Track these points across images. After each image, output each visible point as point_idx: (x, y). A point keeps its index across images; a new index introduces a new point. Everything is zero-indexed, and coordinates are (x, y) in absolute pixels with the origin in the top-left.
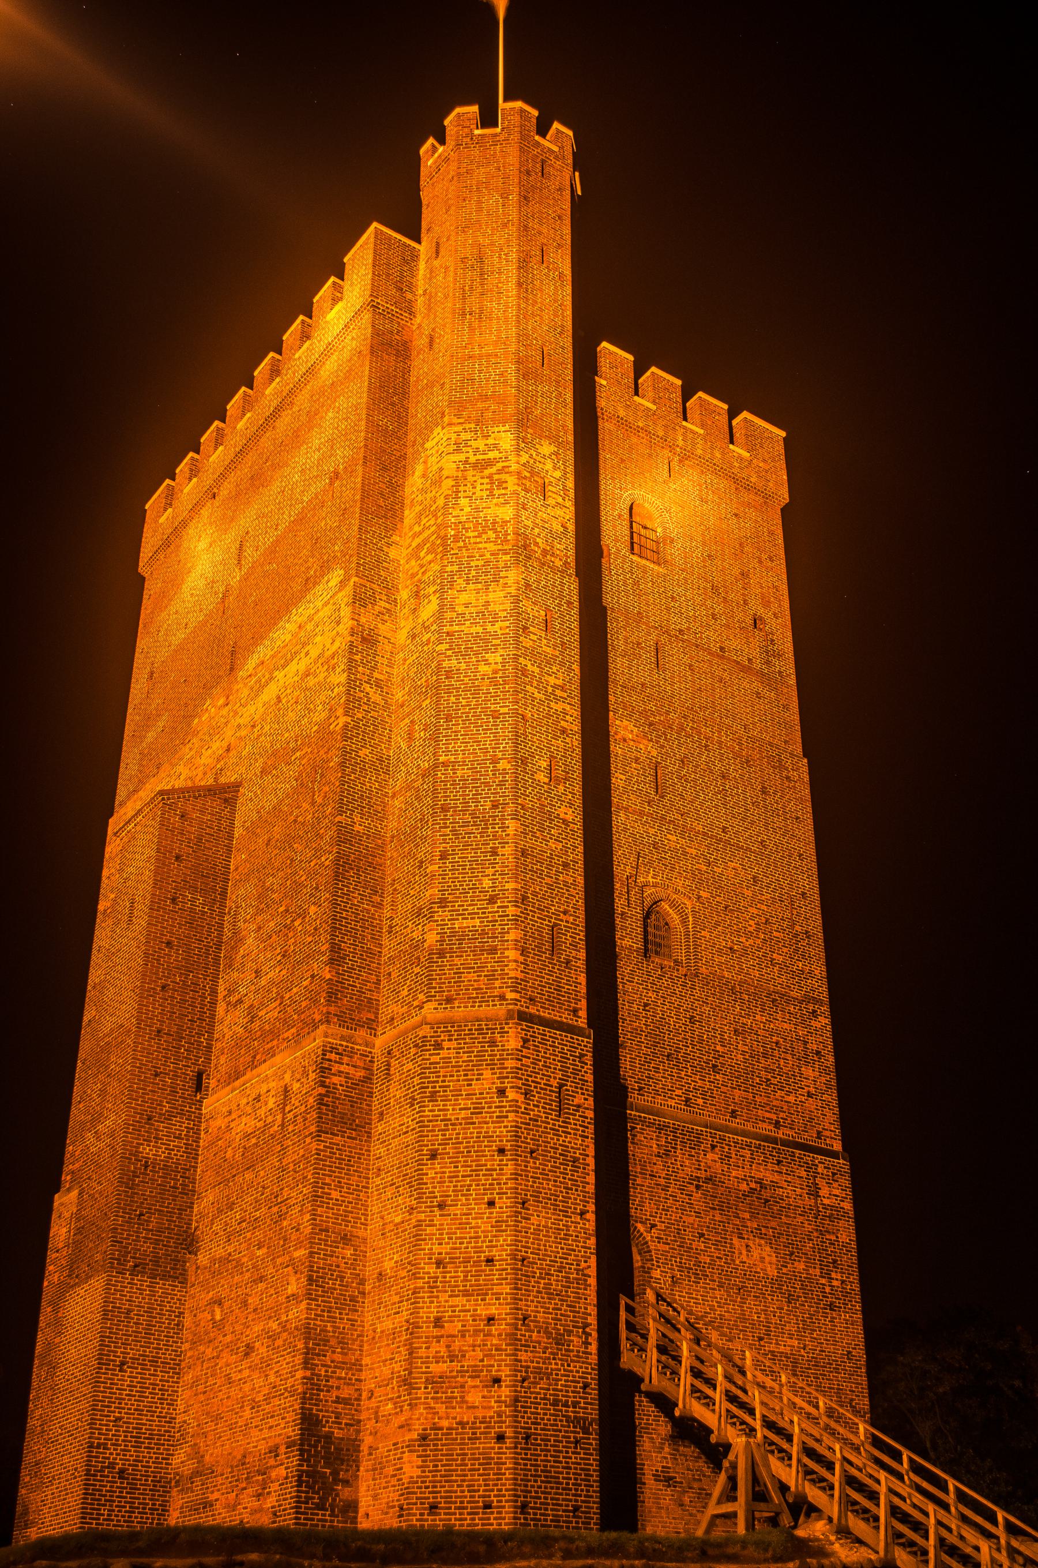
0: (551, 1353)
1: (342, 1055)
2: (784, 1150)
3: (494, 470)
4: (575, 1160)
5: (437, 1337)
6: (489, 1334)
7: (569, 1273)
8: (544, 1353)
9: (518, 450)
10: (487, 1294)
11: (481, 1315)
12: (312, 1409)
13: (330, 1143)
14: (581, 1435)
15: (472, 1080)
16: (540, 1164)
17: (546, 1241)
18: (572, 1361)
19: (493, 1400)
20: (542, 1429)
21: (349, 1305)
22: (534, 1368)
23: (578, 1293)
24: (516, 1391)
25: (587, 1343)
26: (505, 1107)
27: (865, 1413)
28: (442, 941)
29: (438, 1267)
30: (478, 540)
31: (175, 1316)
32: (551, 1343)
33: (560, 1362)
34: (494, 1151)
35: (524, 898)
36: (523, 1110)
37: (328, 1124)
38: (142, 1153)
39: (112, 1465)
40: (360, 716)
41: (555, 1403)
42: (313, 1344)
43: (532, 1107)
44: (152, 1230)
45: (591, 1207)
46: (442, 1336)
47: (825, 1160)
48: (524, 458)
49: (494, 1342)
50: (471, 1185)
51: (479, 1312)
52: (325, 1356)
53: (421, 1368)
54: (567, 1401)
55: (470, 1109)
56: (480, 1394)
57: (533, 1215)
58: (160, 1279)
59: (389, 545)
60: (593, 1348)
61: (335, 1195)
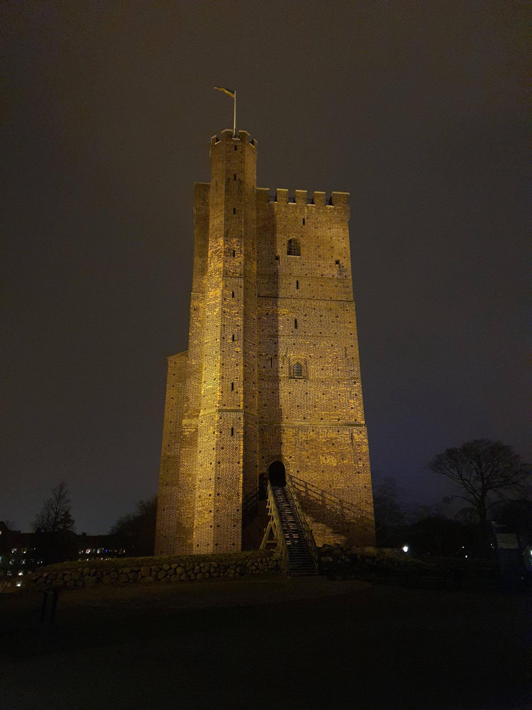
2: (340, 427)
3: (218, 253)
4: (236, 448)
5: (199, 501)
9: (224, 245)
10: (209, 488)
16: (224, 451)
18: (233, 504)
20: (223, 523)
24: (214, 514)
27: (371, 504)
39: (163, 535)
40: (194, 332)
45: (241, 460)
47: (357, 428)
48: (227, 246)
59: (203, 279)
60: (241, 499)
61: (186, 464)
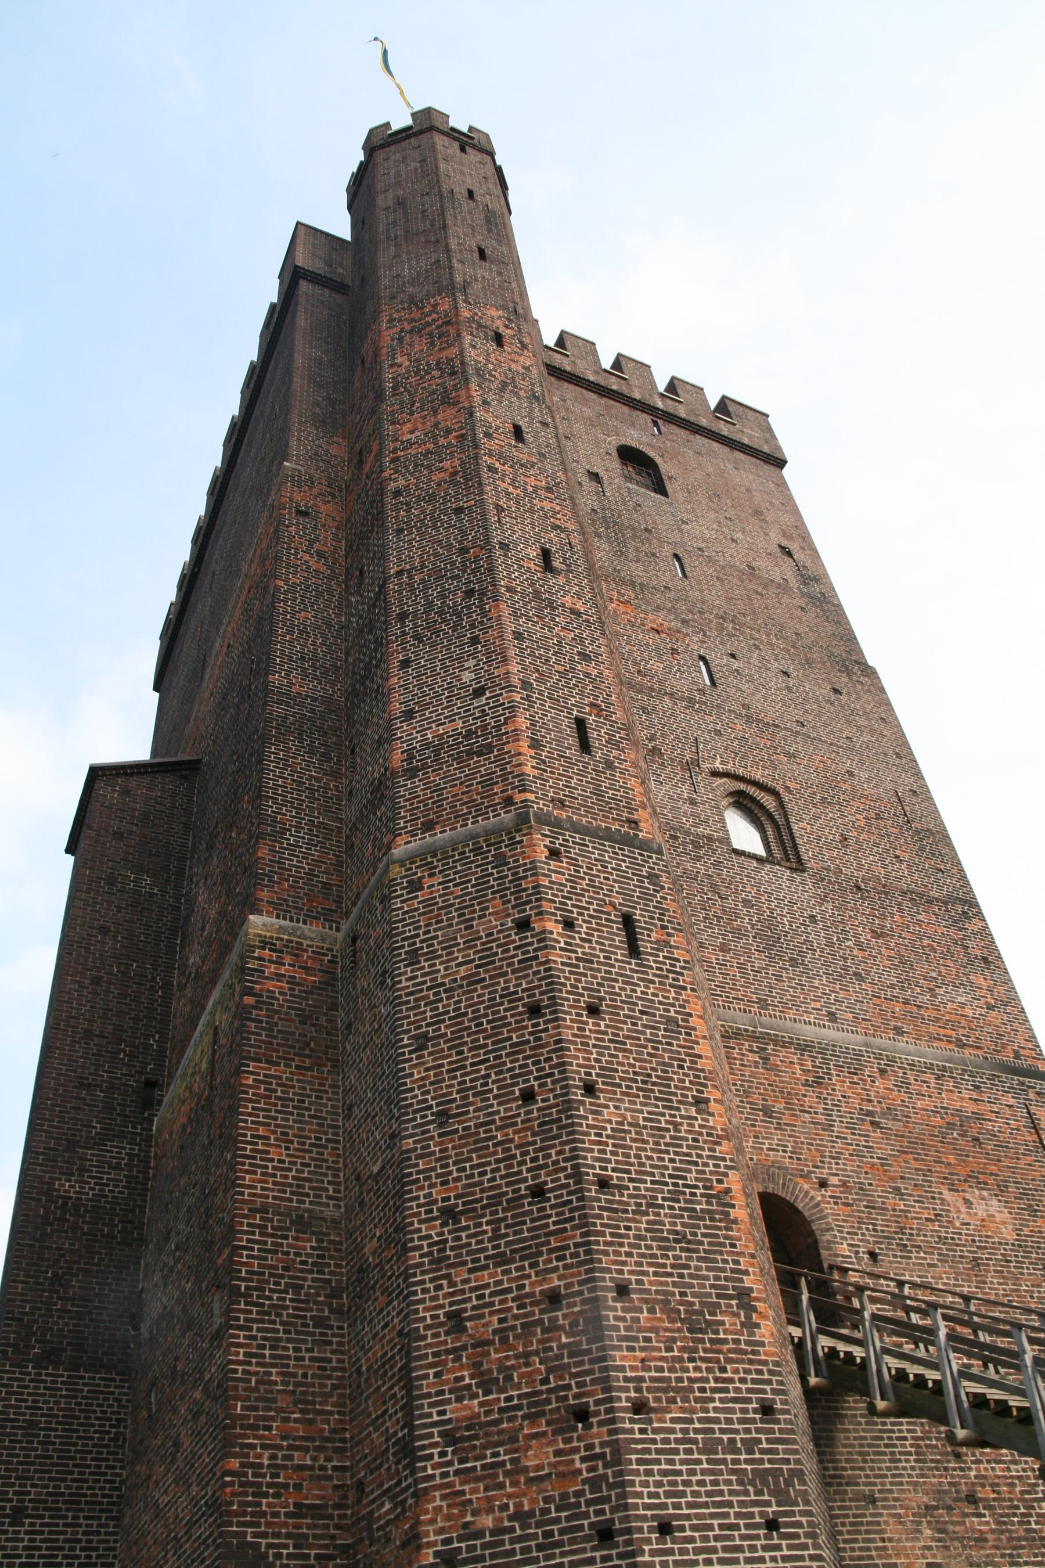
0: (682, 1349)
1: (282, 952)
5: (454, 1350)
6: (553, 1328)
7: (692, 1202)
8: (669, 1349)
10: (540, 1254)
11: (533, 1294)
12: (245, 1534)
13: (265, 1075)
14: (775, 1508)
16: (606, 1026)
17: (638, 1149)
19: (577, 1457)
20: (690, 1505)
21: (313, 1334)
22: (653, 1379)
23: (717, 1236)
25: (751, 1326)
29: (444, 1224)
31: (111, 1426)
32: (679, 1330)
33: (704, 1366)
34: (520, 1014)
36: (562, 945)
37: (260, 1047)
38: (58, 1190)
41: (709, 1448)
42: (243, 1408)
43: (578, 941)
44: (73, 1299)
46: (464, 1348)
49: (564, 1340)
50: (488, 1076)
51: (527, 1289)
52: (269, 1428)
53: (430, 1415)
54: (732, 1441)
56: (550, 1450)
57: (607, 1107)
58: (86, 1371)
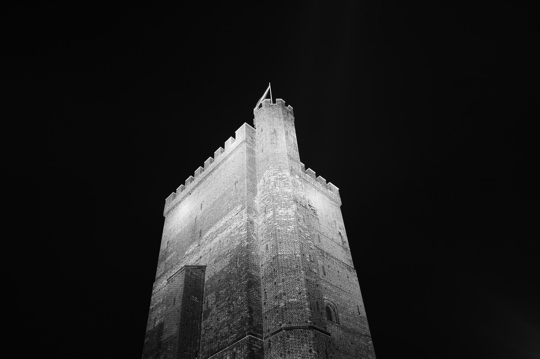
3: (285, 180)
15: (301, 347)
26: (312, 356)
28: (285, 305)
30: (283, 197)
35: (309, 293)
48: (292, 178)
55: (301, 356)
59: (254, 199)
